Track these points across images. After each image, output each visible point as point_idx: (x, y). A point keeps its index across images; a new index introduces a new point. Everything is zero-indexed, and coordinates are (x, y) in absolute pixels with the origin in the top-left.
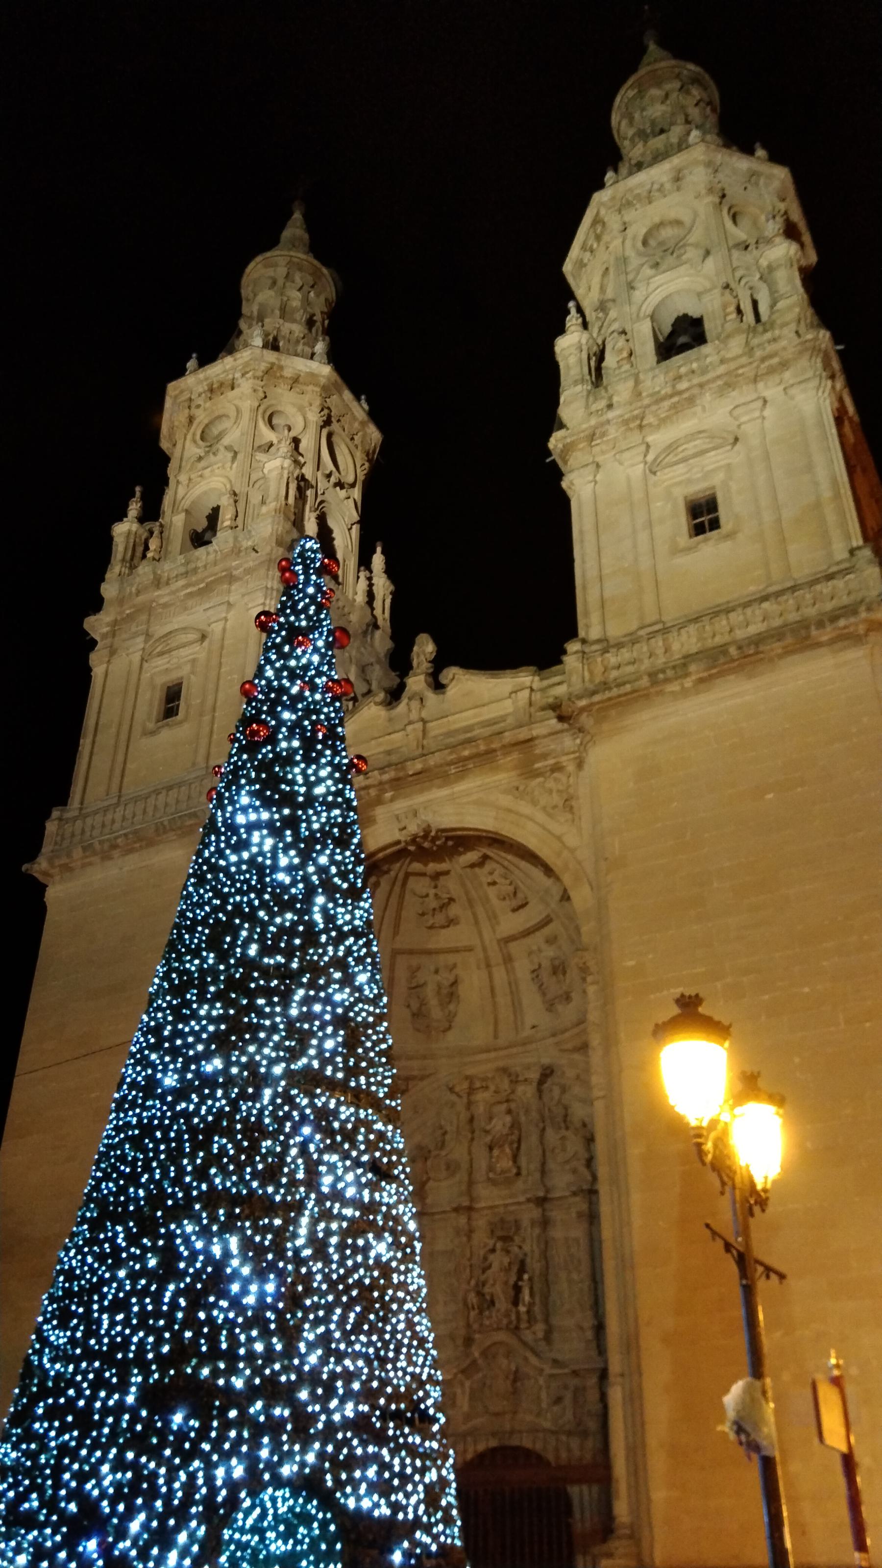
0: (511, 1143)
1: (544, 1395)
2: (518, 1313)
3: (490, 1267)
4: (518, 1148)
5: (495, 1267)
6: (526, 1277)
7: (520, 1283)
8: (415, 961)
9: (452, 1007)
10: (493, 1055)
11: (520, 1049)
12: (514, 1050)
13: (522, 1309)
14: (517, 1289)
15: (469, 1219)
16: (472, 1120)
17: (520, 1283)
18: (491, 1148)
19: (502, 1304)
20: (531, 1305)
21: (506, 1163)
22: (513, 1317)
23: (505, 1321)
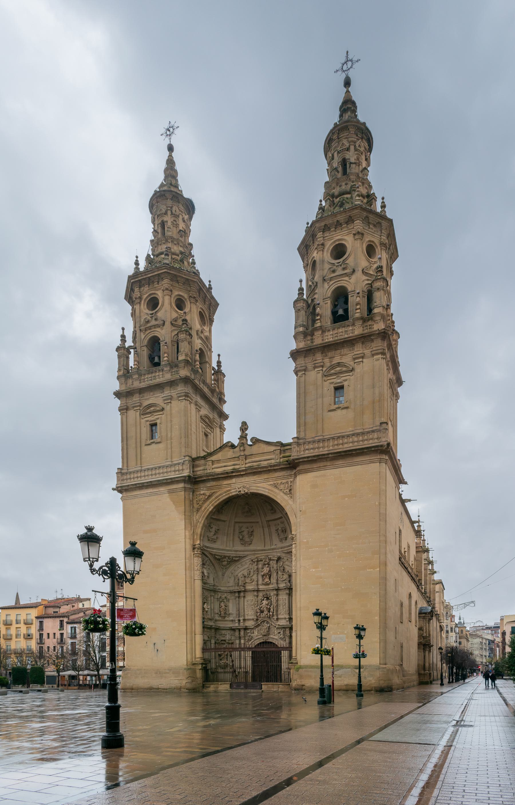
1: (276, 631)
2: (270, 614)
3: (263, 604)
4: (271, 576)
5: (264, 604)
8: (241, 525)
9: (252, 538)
10: (264, 552)
11: (272, 551)
12: (270, 551)
13: (271, 613)
14: (270, 609)
16: (257, 569)
18: (263, 576)
19: (266, 612)
21: (267, 580)
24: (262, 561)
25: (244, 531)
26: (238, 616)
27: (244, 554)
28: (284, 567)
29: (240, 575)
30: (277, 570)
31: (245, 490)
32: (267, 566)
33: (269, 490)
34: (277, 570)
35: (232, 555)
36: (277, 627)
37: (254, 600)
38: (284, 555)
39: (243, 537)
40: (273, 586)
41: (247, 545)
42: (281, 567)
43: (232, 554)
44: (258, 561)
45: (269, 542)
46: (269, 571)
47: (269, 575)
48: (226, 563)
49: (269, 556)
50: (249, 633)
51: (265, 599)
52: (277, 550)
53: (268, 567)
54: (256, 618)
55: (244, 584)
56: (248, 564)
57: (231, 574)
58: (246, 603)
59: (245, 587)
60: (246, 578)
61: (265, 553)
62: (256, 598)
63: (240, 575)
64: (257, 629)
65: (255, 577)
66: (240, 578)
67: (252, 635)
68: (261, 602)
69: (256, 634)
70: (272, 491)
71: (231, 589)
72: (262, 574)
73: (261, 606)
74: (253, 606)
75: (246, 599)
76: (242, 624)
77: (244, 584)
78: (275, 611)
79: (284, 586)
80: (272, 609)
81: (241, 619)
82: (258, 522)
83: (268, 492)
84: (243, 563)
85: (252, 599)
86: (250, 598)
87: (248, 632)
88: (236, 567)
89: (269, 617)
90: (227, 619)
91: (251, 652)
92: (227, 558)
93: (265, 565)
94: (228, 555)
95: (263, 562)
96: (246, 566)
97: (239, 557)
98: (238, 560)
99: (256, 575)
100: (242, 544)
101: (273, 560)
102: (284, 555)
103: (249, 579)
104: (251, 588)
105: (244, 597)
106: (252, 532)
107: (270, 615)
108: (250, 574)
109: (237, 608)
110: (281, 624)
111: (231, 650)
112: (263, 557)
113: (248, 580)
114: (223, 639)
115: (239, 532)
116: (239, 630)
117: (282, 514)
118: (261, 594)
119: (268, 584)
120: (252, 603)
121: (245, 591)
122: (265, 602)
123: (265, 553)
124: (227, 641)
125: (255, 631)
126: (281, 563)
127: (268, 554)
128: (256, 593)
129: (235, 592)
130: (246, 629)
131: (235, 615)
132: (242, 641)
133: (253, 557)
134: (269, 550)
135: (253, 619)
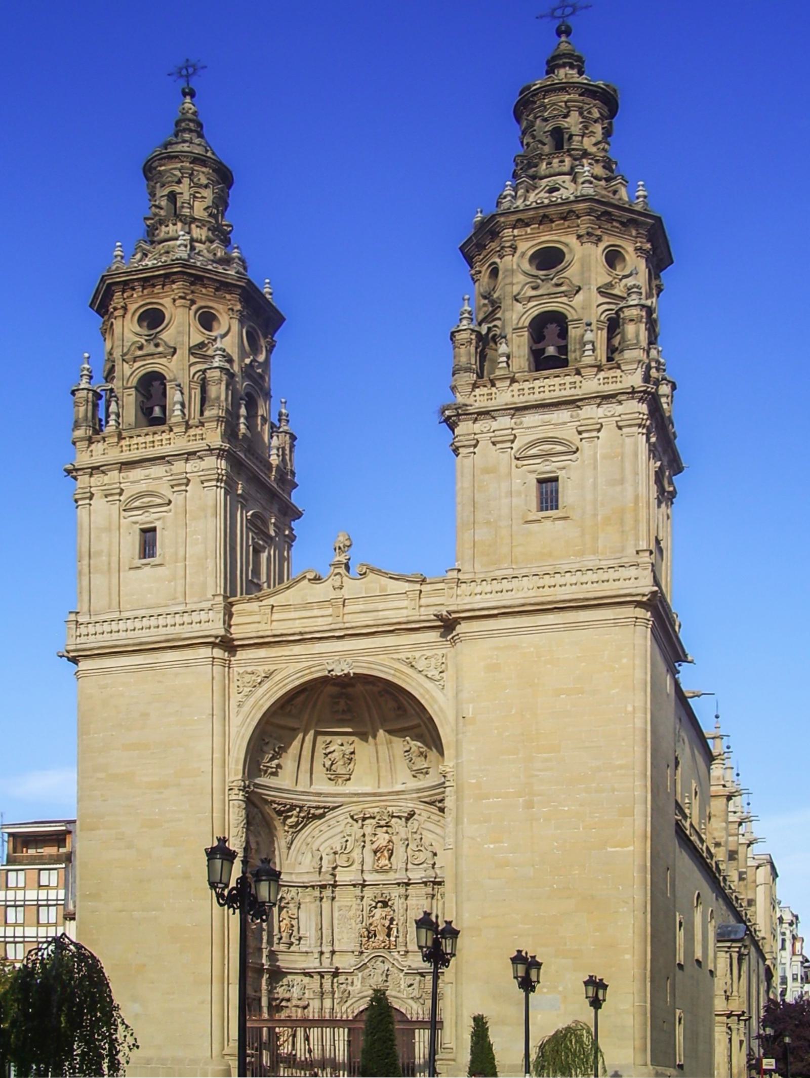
0: (389, 850)
1: (402, 982)
2: (389, 940)
3: (373, 916)
5: (377, 916)
6: (395, 923)
7: (392, 926)
9: (351, 766)
13: (393, 939)
14: (389, 929)
15: (362, 891)
16: (364, 835)
17: (392, 926)
18: (375, 852)
19: (381, 937)
20: (397, 937)
21: (384, 862)
22: (387, 942)
23: (383, 945)
24: (374, 818)
25: (334, 751)
26: (319, 944)
27: (334, 802)
28: (421, 834)
29: (325, 850)
30: (407, 839)
34: (407, 839)
35: (309, 804)
36: (406, 971)
37: (355, 907)
38: (422, 807)
39: (332, 764)
40: (397, 876)
41: (340, 781)
42: (416, 833)
43: (310, 801)
44: (364, 819)
45: (390, 777)
46: (389, 841)
47: (389, 850)
48: (294, 819)
49: (390, 809)
50: (342, 984)
51: (380, 905)
53: (387, 832)
54: (359, 949)
55: (334, 868)
56: (343, 825)
57: (304, 847)
58: (336, 914)
59: (334, 875)
60: (337, 856)
61: (380, 801)
62: (359, 901)
63: (325, 850)
64: (360, 974)
65: (356, 855)
66: (324, 856)
67: (350, 988)
68: (371, 911)
69: (359, 986)
70: (402, 672)
71: (305, 879)
72: (375, 846)
73: (371, 921)
74: (353, 921)
75: (336, 904)
76: (326, 961)
77: (334, 868)
78: (401, 935)
79: (422, 878)
80: (395, 930)
81: (327, 949)
83: (394, 675)
84: (332, 822)
85: (349, 904)
86: (346, 898)
87: (340, 982)
88: (317, 830)
89: (389, 948)
90: (292, 949)
91: (346, 1030)
92: (298, 809)
94: (300, 803)
95: (376, 820)
96: (339, 829)
97: (325, 808)
98: (322, 816)
99: (358, 851)
100: (330, 779)
101: (399, 817)
102: (422, 807)
103: (344, 857)
104: (348, 879)
105: (333, 898)
106: (353, 753)
107: (390, 943)
108: (346, 848)
109: (317, 925)
110: (413, 966)
111: (309, 1024)
112: (377, 810)
113: (341, 860)
114: (287, 995)
115: (327, 755)
116: (322, 977)
117: (421, 718)
118: (369, 893)
119: (386, 872)
120: (352, 913)
121: (334, 886)
122: (379, 912)
123: (380, 801)
124: (294, 1002)
125: (355, 981)
126: (416, 824)
128: (358, 891)
129: (313, 887)
130: (336, 974)
131: (313, 942)
132: (328, 1003)
133: (355, 809)
135: (353, 952)
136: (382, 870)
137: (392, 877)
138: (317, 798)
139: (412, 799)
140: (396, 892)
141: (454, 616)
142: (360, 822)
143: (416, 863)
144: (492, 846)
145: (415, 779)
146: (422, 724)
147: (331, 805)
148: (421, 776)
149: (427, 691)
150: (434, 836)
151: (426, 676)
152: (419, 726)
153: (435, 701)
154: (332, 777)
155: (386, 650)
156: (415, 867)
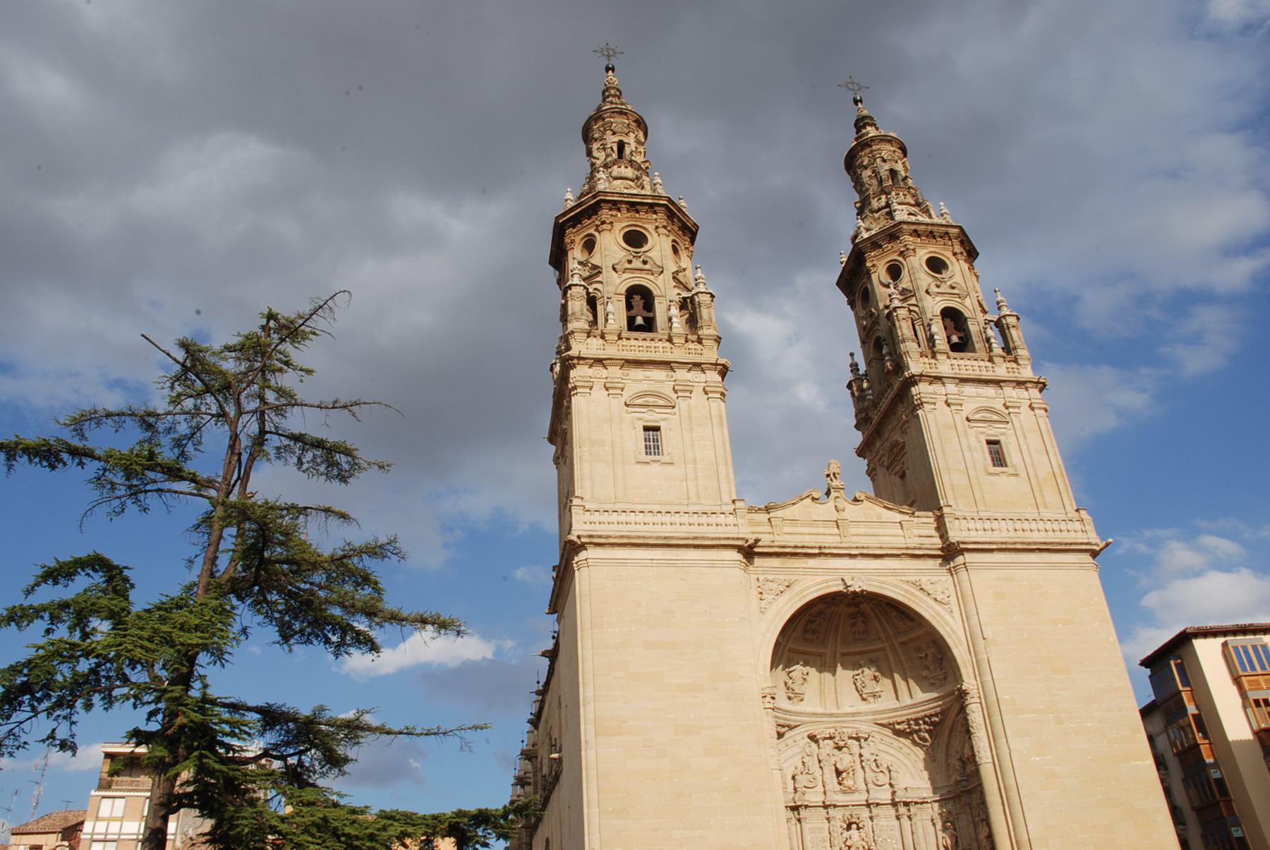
12: (847, 719)
18: (838, 773)
27: (796, 721)
31: (861, 584)
32: (845, 749)
33: (906, 591)
41: (795, 700)
49: (850, 730)
52: (863, 718)
58: (808, 837)
61: (836, 722)
70: (912, 594)
82: (820, 655)
93: (839, 748)
96: (797, 749)
97: (788, 726)
100: (790, 698)
101: (858, 739)
102: (875, 729)
106: (807, 674)
123: (836, 722)
127: (843, 725)
128: (832, 811)
134: (847, 714)
136: (850, 791)
137: (861, 798)
138: (785, 716)
139: (866, 721)
140: (865, 813)
141: (962, 546)
142: (821, 742)
143: (880, 784)
144: (1038, 759)
145: (864, 702)
146: (888, 649)
147: (793, 724)
148: (871, 699)
149: (938, 614)
150: (889, 758)
151: (936, 600)
152: (883, 649)
153: (947, 624)
154: (792, 696)
155: (894, 572)
156: (878, 788)
